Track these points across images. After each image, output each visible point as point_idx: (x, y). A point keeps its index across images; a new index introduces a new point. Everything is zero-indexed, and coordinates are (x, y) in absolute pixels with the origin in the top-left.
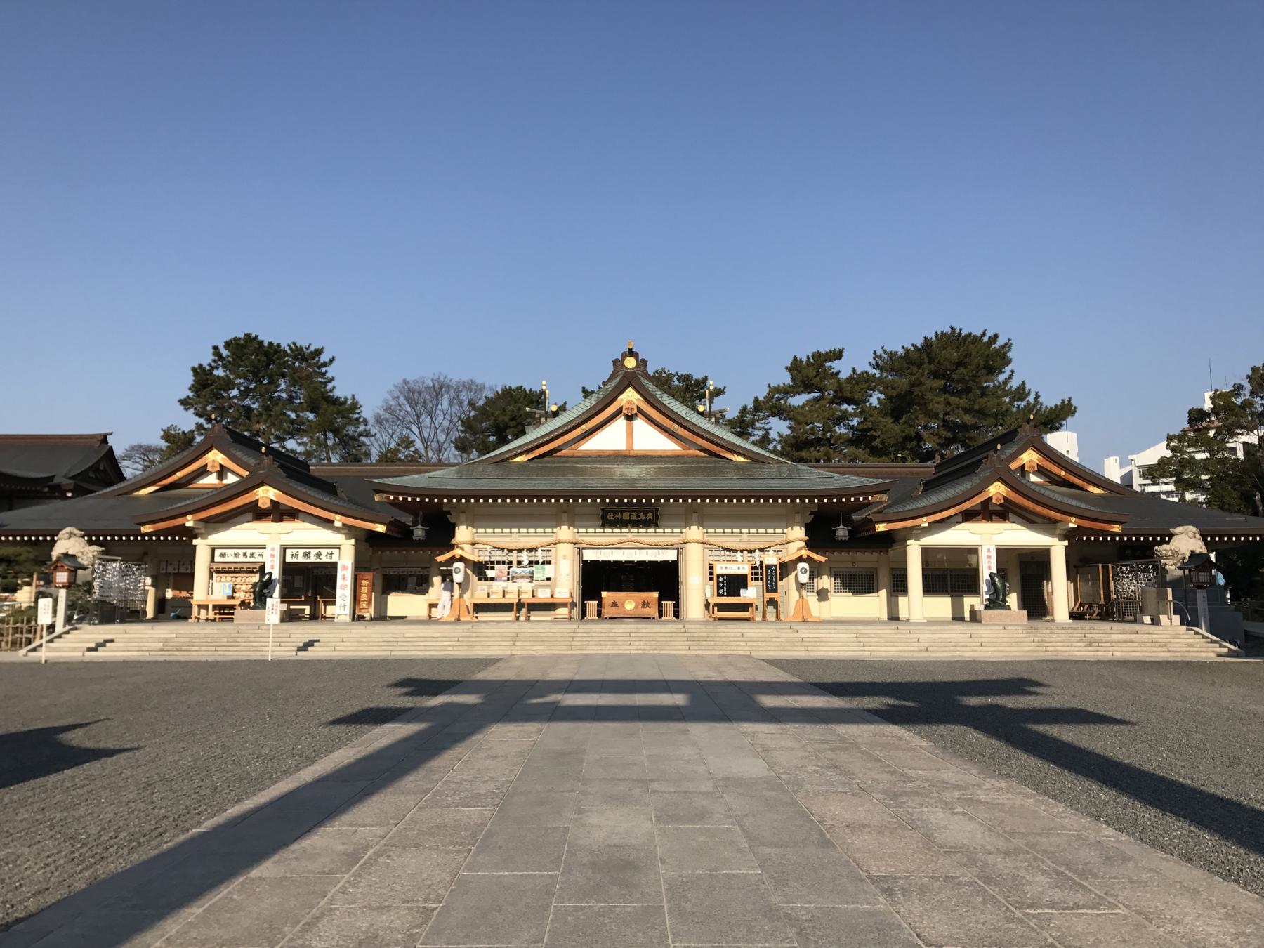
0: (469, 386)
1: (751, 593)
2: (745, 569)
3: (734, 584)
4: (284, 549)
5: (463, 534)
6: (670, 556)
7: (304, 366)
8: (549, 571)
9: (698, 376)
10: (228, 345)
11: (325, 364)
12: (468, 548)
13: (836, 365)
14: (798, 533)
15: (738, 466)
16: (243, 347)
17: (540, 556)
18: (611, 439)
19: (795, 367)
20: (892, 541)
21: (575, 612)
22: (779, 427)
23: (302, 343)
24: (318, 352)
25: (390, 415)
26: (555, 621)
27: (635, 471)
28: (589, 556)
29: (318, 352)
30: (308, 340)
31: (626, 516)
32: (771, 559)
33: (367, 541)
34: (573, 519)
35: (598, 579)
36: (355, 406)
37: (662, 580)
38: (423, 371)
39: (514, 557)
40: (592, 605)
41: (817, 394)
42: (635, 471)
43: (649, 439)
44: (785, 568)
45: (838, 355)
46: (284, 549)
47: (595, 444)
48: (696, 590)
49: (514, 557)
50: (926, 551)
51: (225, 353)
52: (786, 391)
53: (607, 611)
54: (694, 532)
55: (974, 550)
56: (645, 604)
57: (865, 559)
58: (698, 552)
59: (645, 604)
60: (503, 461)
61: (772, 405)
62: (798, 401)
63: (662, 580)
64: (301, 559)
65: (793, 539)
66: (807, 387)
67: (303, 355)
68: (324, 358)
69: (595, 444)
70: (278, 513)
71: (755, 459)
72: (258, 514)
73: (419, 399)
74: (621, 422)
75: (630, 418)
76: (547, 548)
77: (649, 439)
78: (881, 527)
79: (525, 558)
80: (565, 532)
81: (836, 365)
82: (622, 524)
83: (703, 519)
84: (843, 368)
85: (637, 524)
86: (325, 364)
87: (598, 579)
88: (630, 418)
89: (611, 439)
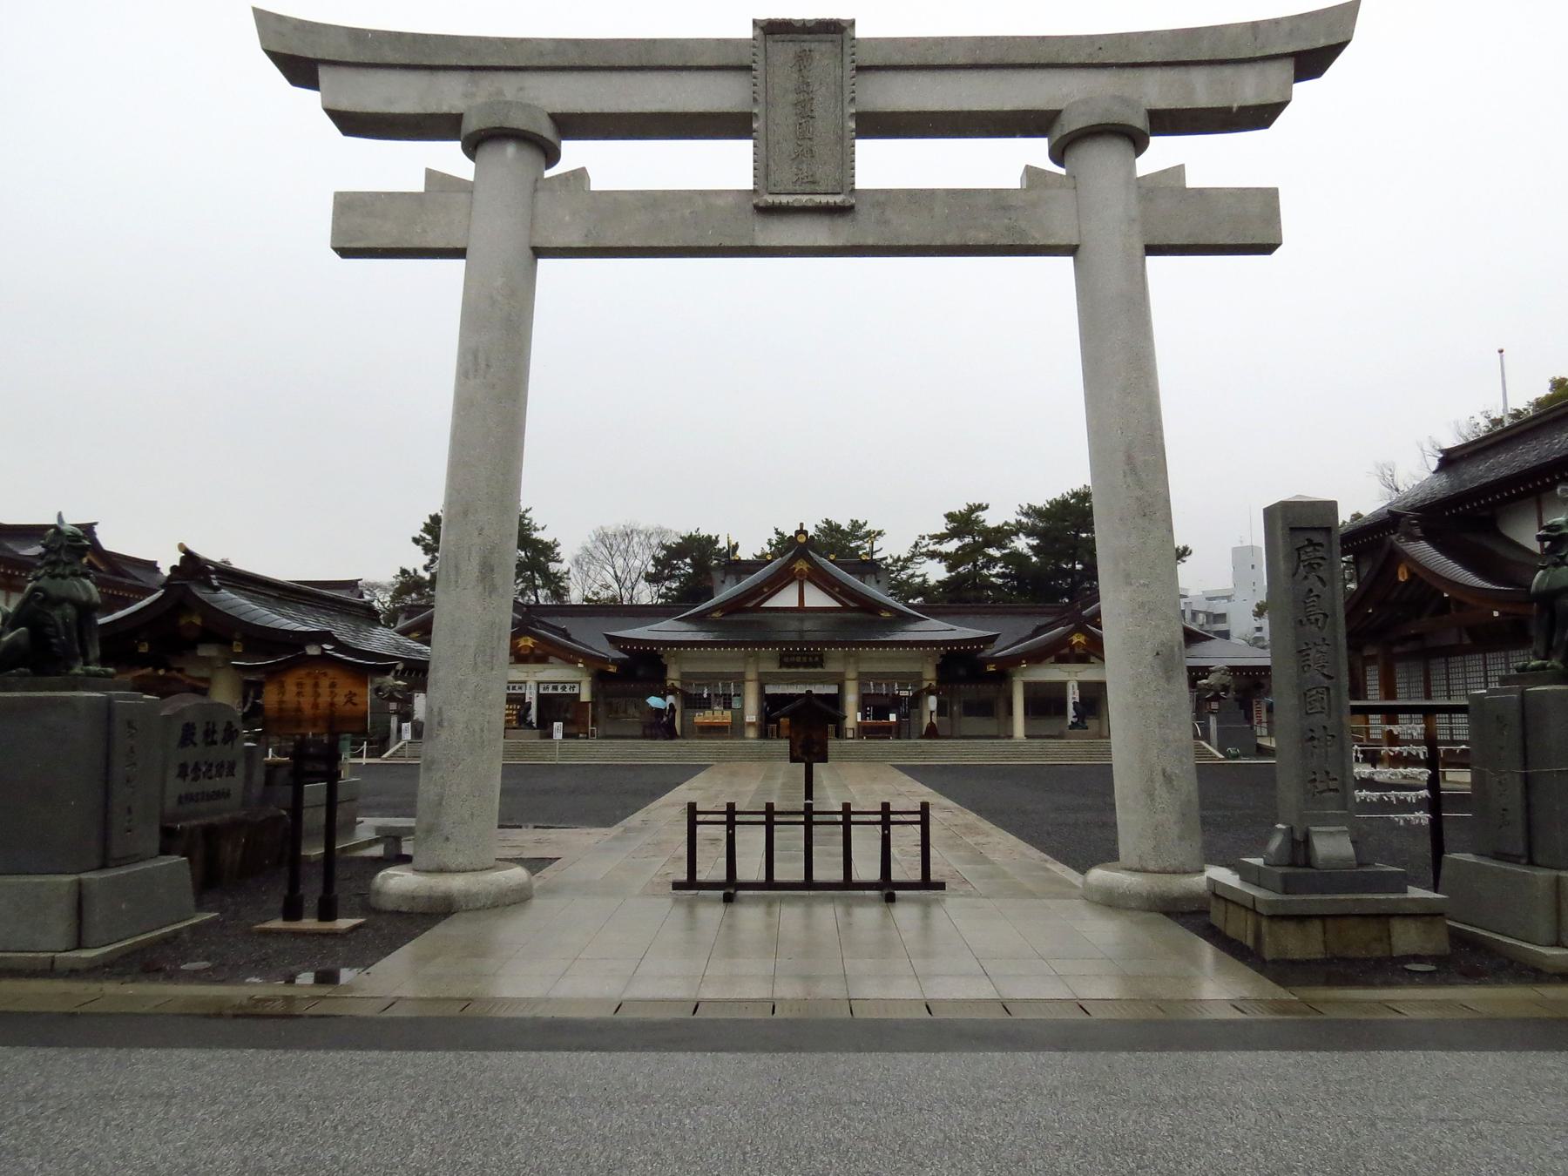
4: (539, 683)
6: (833, 690)
13: (982, 515)
18: (787, 598)
20: (1002, 677)
25: (586, 559)
28: (770, 690)
31: (798, 659)
33: (601, 678)
38: (614, 522)
41: (968, 540)
43: (816, 598)
46: (539, 683)
50: (1027, 685)
52: (941, 538)
55: (1063, 686)
57: (988, 690)
64: (550, 691)
73: (611, 542)
77: (816, 598)
81: (982, 515)
84: (991, 519)
89: (787, 598)
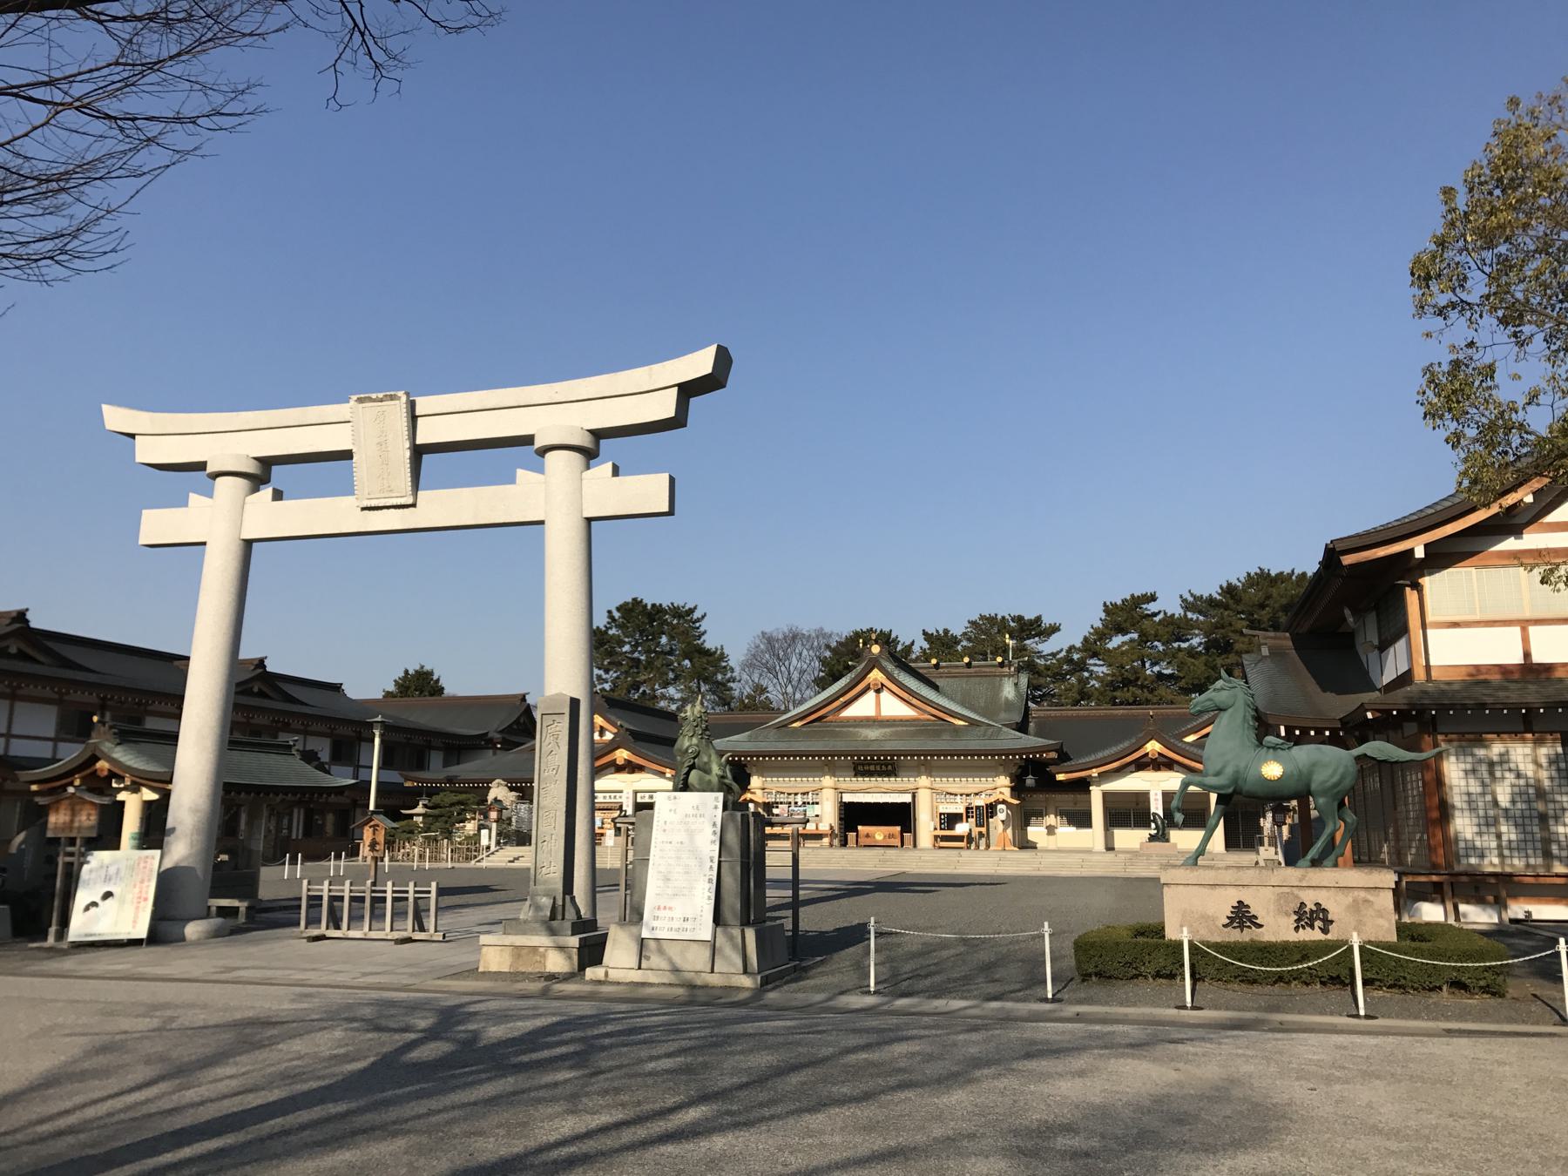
0: (821, 634)
1: (961, 829)
2: (961, 810)
3: (951, 820)
4: (636, 793)
5: (755, 782)
6: (907, 798)
7: (682, 622)
8: (817, 809)
9: (1029, 616)
10: (618, 609)
11: (698, 620)
12: (759, 792)
13: (1152, 607)
14: (1003, 781)
15: (956, 729)
16: (631, 610)
17: (810, 798)
18: (863, 707)
19: (1110, 610)
20: (1083, 786)
21: (836, 842)
22: (1099, 668)
23: (678, 602)
24: (691, 611)
26: (822, 847)
27: (873, 734)
28: (847, 798)
29: (691, 611)
30: (681, 599)
32: (980, 802)
34: (833, 770)
35: (854, 816)
36: (722, 657)
37: (901, 816)
38: (778, 625)
39: (791, 799)
40: (852, 835)
42: (873, 734)
43: (893, 707)
44: (991, 809)
45: (1153, 598)
46: (636, 793)
47: (853, 711)
48: (926, 825)
49: (791, 799)
50: (1105, 795)
51: (617, 615)
53: (862, 841)
54: (924, 781)
56: (891, 836)
58: (931, 797)
59: (891, 836)
60: (784, 725)
61: (1093, 646)
62: (1116, 641)
63: (901, 816)
65: (1000, 786)
66: (1122, 631)
67: (677, 612)
68: (696, 615)
69: (853, 711)
70: (630, 768)
71: (973, 723)
72: (619, 769)
73: (775, 649)
74: (871, 694)
75: (878, 691)
76: (817, 792)
77: (893, 707)
78: (1060, 777)
79: (799, 799)
80: (828, 781)
81: (1152, 607)
82: (870, 774)
83: (929, 770)
85: (882, 774)
86: (698, 620)
87: (854, 816)
88: (878, 691)
89: (863, 707)
